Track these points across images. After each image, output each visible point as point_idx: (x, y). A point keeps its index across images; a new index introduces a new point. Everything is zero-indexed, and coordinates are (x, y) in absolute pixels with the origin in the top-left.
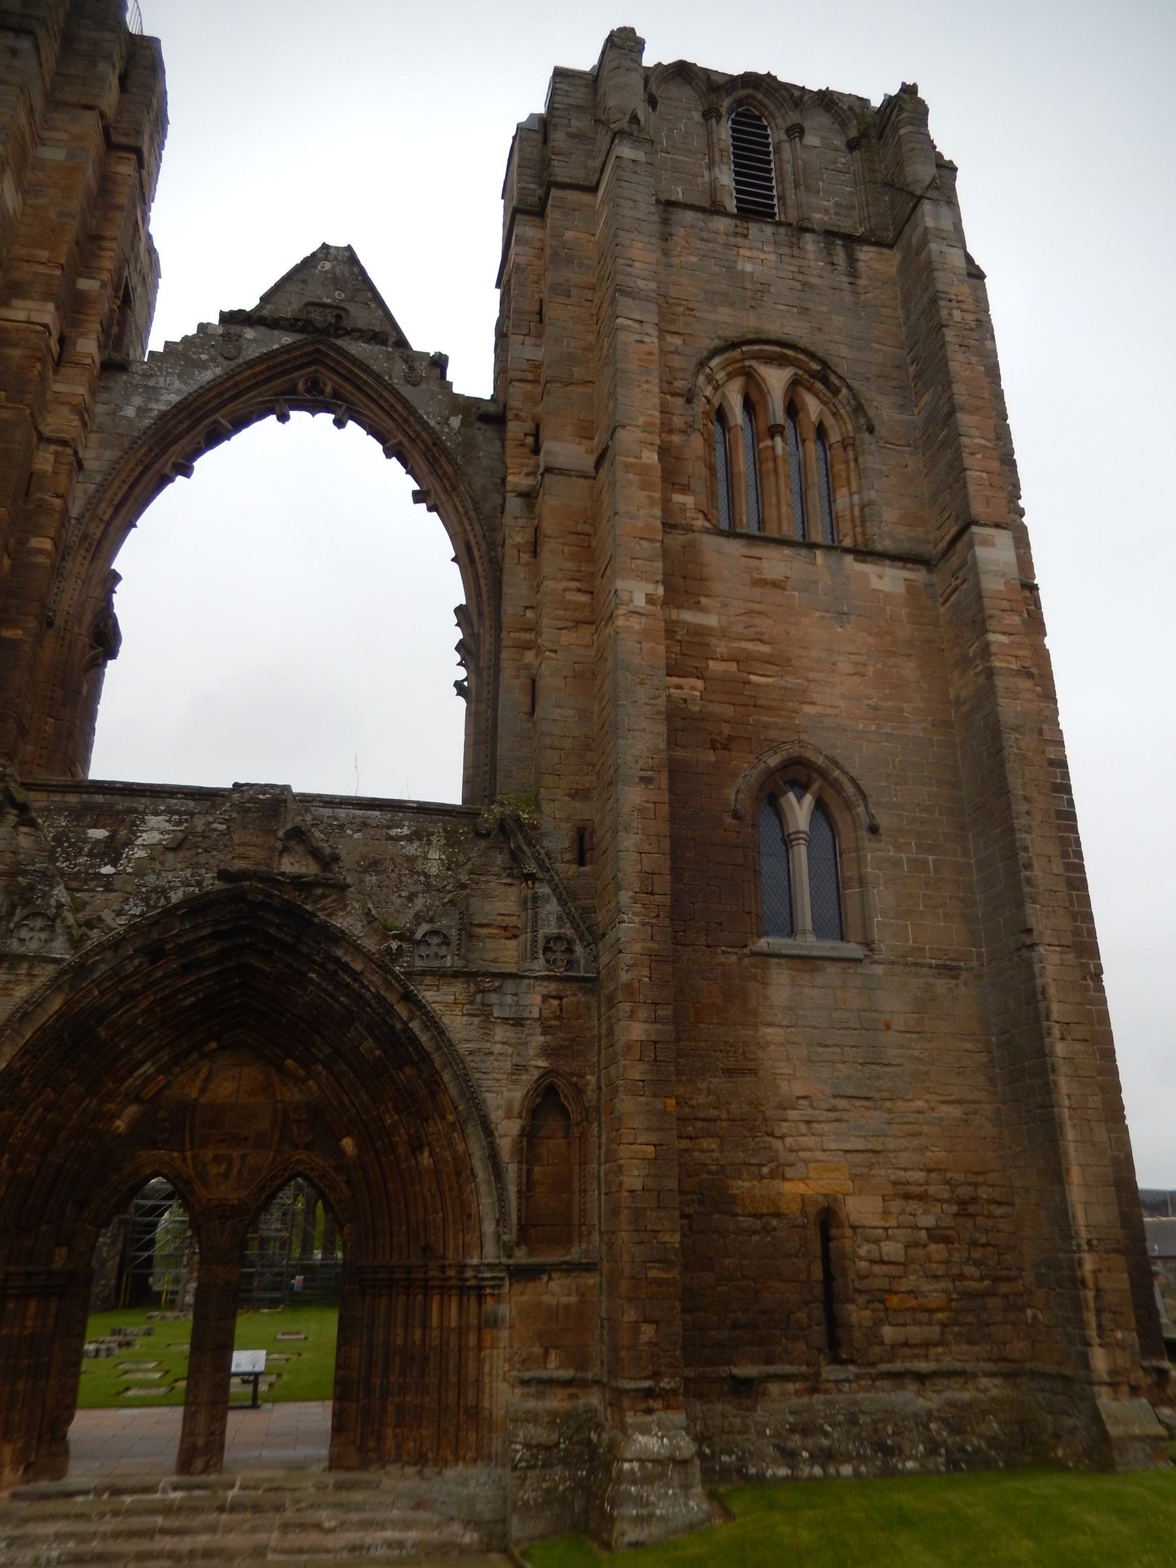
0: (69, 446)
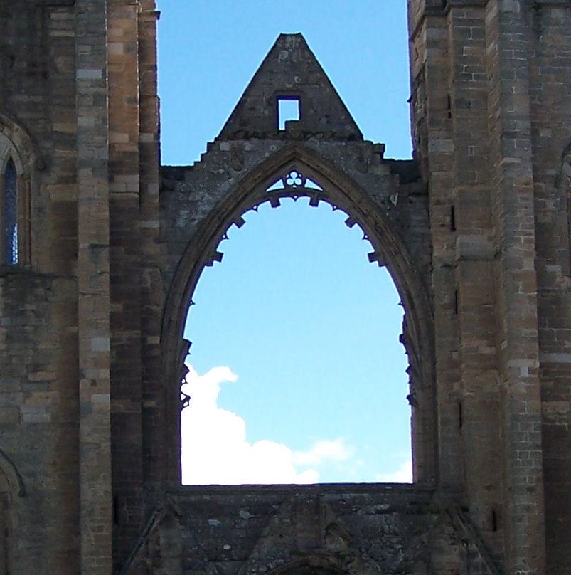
0: (157, 267)
